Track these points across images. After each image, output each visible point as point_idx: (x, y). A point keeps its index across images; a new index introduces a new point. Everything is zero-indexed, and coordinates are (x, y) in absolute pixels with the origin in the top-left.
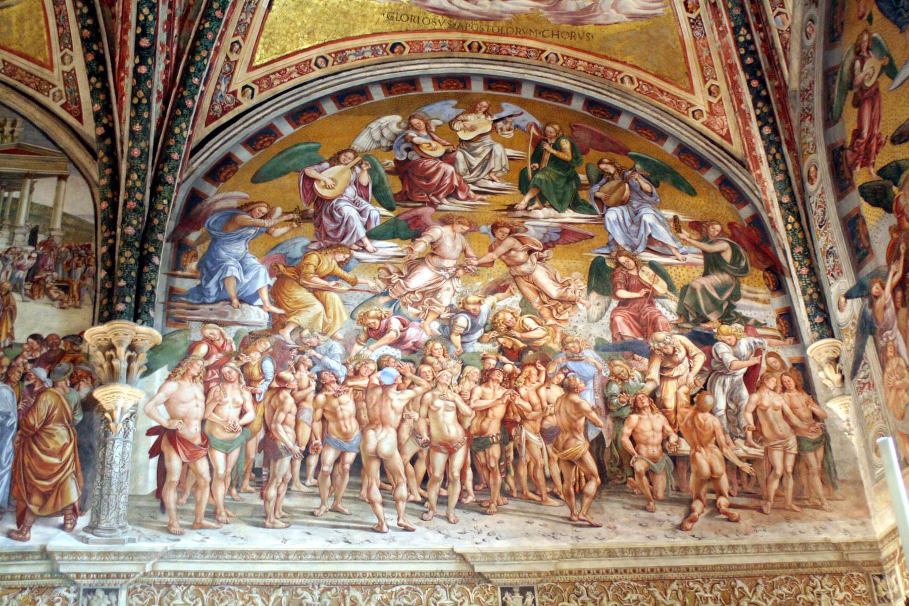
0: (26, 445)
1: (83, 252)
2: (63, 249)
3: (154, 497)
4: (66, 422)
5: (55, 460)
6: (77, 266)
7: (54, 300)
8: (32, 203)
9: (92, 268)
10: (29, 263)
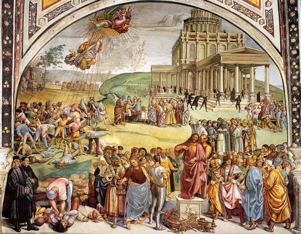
0: (268, 193)
1: (280, 104)
2: (272, 103)
4: (282, 184)
5: (280, 200)
6: (278, 111)
8: (256, 80)
9: (285, 112)
10: (258, 111)
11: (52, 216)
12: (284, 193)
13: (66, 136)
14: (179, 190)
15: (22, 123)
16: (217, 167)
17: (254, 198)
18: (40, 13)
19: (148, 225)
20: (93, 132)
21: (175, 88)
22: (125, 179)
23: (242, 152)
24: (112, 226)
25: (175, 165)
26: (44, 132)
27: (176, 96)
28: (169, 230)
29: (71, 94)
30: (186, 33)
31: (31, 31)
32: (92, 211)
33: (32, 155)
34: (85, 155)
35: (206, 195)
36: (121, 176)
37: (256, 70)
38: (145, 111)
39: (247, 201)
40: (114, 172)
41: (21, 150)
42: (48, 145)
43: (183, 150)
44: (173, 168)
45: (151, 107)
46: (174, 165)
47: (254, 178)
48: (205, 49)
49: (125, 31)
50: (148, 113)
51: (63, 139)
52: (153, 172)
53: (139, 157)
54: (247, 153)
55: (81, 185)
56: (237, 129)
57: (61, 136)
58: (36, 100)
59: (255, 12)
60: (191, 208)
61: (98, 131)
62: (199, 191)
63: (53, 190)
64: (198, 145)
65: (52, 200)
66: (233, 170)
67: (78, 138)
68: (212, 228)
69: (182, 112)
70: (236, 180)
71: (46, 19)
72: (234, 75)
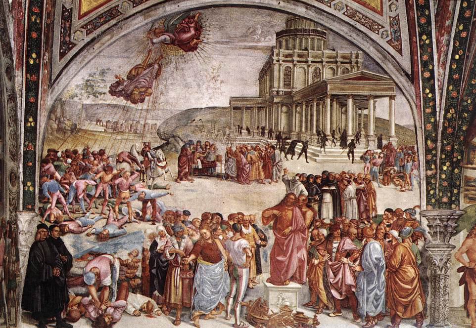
2: (398, 150)
3: (463, 309)
4: (412, 264)
6: (408, 161)
7: (397, 186)
10: (380, 161)
11: (91, 309)
12: (415, 276)
13: (111, 195)
15: (50, 179)
16: (320, 240)
17: (373, 283)
18: (76, 22)
20: (146, 190)
21: (263, 129)
22: (193, 257)
24: (174, 323)
26: (80, 191)
27: (264, 140)
29: (117, 138)
30: (279, 52)
31: (64, 48)
32: (147, 301)
33: (64, 223)
34: (137, 222)
35: (305, 279)
36: (188, 253)
37: (376, 104)
38: (221, 161)
39: (362, 288)
40: (177, 246)
41: (49, 216)
42: (86, 209)
43: (274, 215)
44: (259, 242)
45: (230, 156)
47: (373, 255)
48: (306, 73)
49: (194, 48)
50: (225, 165)
51: (106, 200)
55: (131, 264)
57: (104, 196)
58: (70, 147)
59: (376, 20)
61: (156, 190)
62: (295, 274)
63: (93, 272)
64: (294, 209)
65: (90, 286)
66: (344, 244)
67: (127, 200)
69: (273, 163)
70: (347, 258)
71: (84, 31)
72: (346, 111)
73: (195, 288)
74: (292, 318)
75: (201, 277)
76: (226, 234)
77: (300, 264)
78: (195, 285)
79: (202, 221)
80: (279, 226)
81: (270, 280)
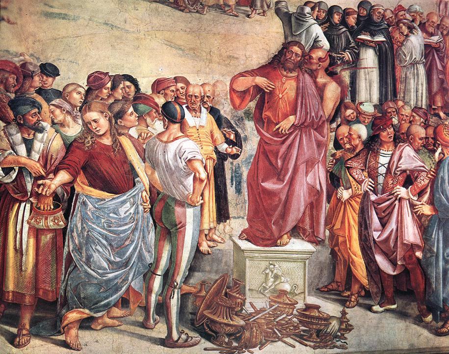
14: (243, 218)
16: (354, 148)
19: (143, 332)
22: (63, 177)
23: (424, 107)
25: (232, 137)
28: (209, 345)
35: (324, 232)
40: (22, 149)
43: (258, 89)
44: (224, 147)
46: (227, 136)
52: (161, 158)
53: (113, 103)
54: (437, 112)
56: (412, 38)
60: (280, 274)
62: (302, 220)
64: (301, 77)
66: (400, 158)
68: (339, 334)
70: (407, 188)
73: (69, 252)
74: (295, 319)
75: (83, 228)
76: (148, 126)
77: (313, 199)
78: (69, 247)
79: (88, 92)
80: (268, 113)
81: (248, 235)
